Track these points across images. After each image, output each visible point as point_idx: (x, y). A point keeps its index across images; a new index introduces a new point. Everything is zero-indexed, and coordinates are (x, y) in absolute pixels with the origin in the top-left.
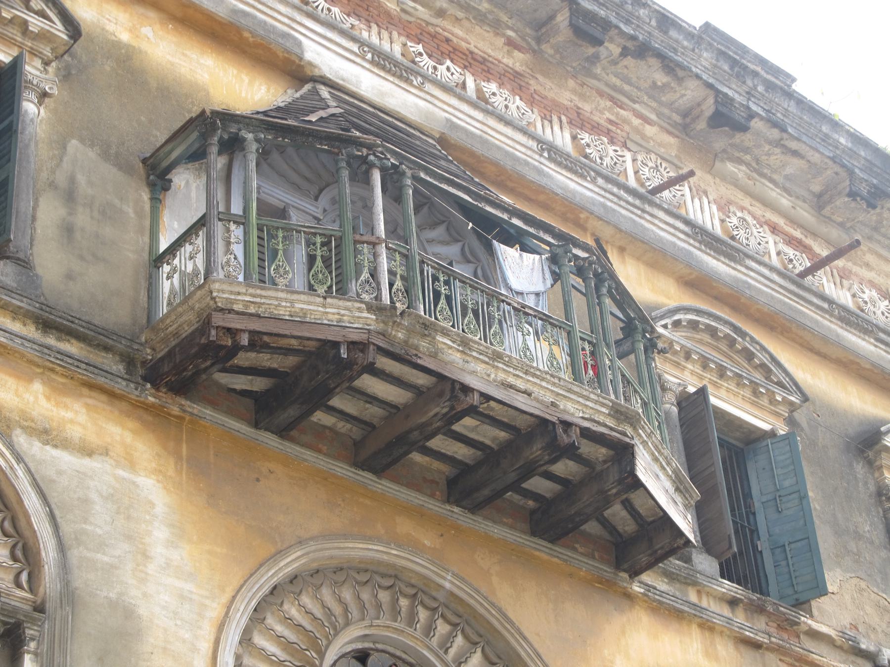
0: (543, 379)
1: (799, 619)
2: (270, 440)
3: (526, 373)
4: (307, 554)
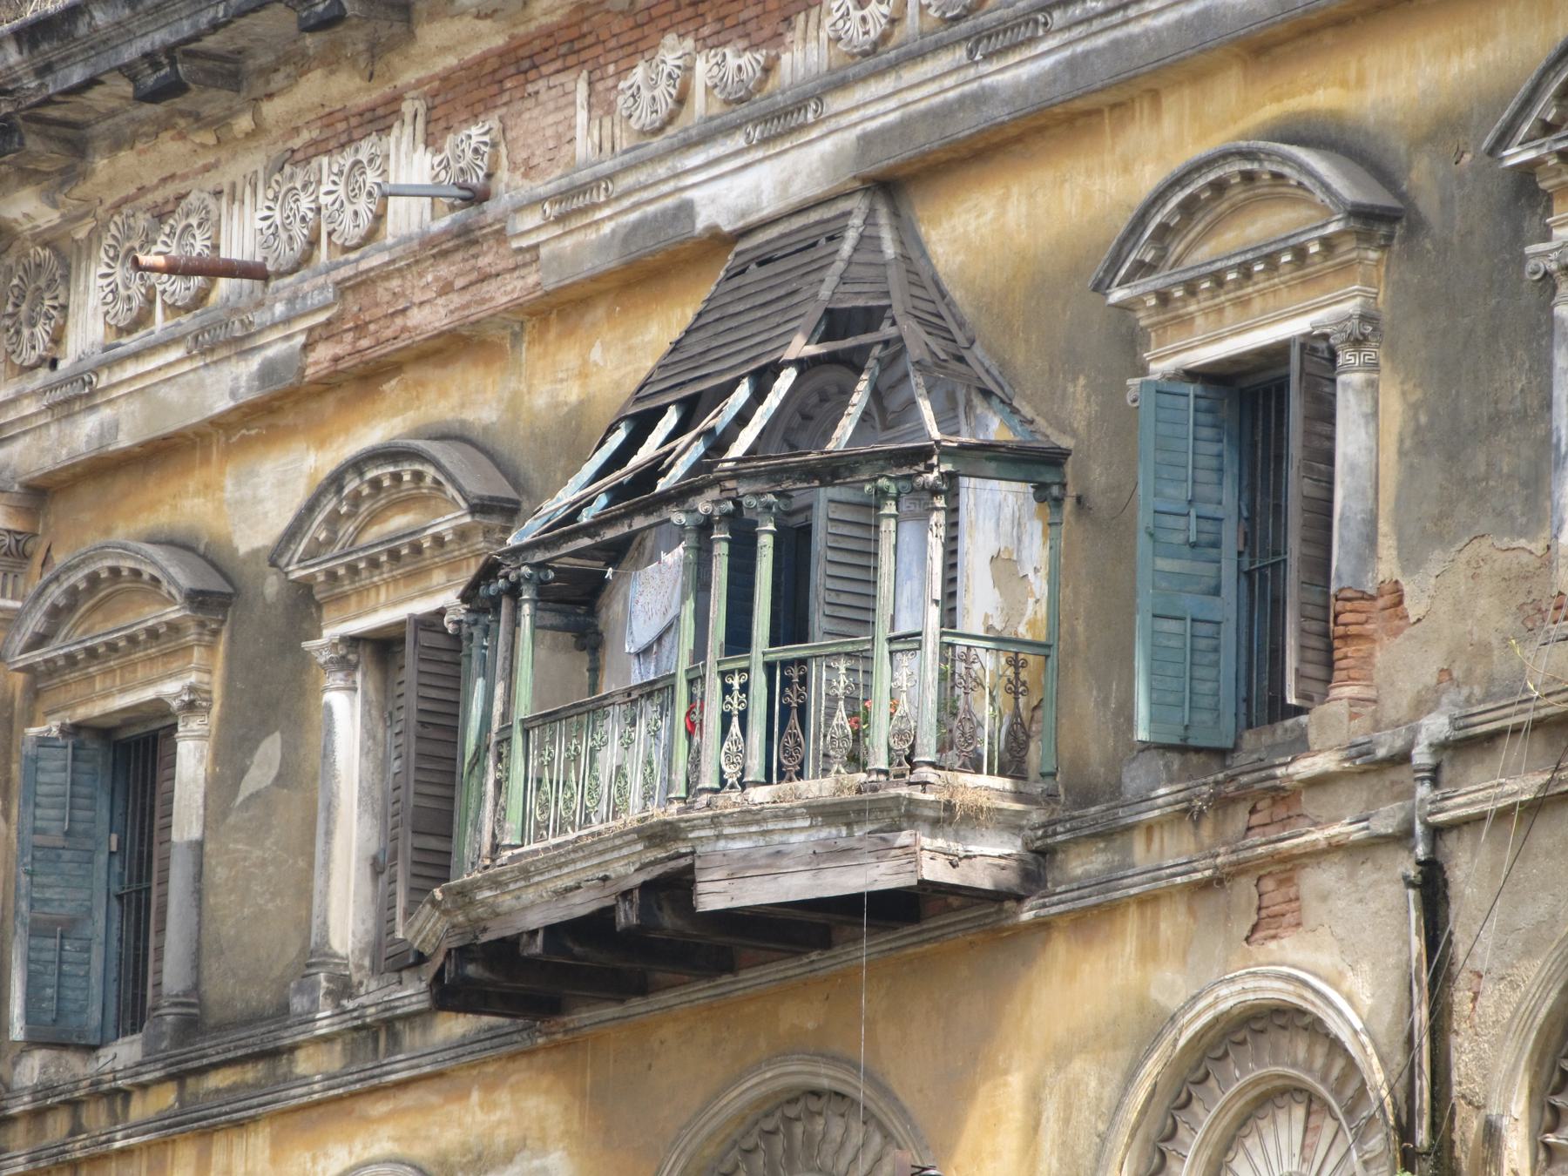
0: (574, 861)
1: (1275, 778)
2: (637, 1005)
3: (559, 867)
4: (683, 1151)
